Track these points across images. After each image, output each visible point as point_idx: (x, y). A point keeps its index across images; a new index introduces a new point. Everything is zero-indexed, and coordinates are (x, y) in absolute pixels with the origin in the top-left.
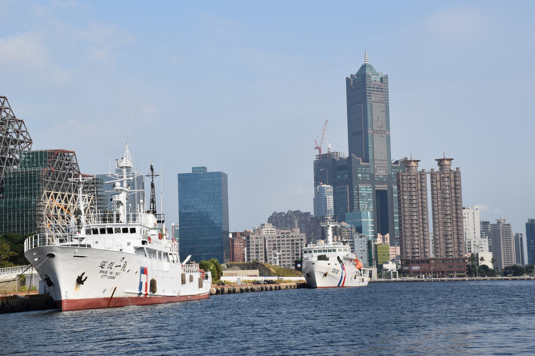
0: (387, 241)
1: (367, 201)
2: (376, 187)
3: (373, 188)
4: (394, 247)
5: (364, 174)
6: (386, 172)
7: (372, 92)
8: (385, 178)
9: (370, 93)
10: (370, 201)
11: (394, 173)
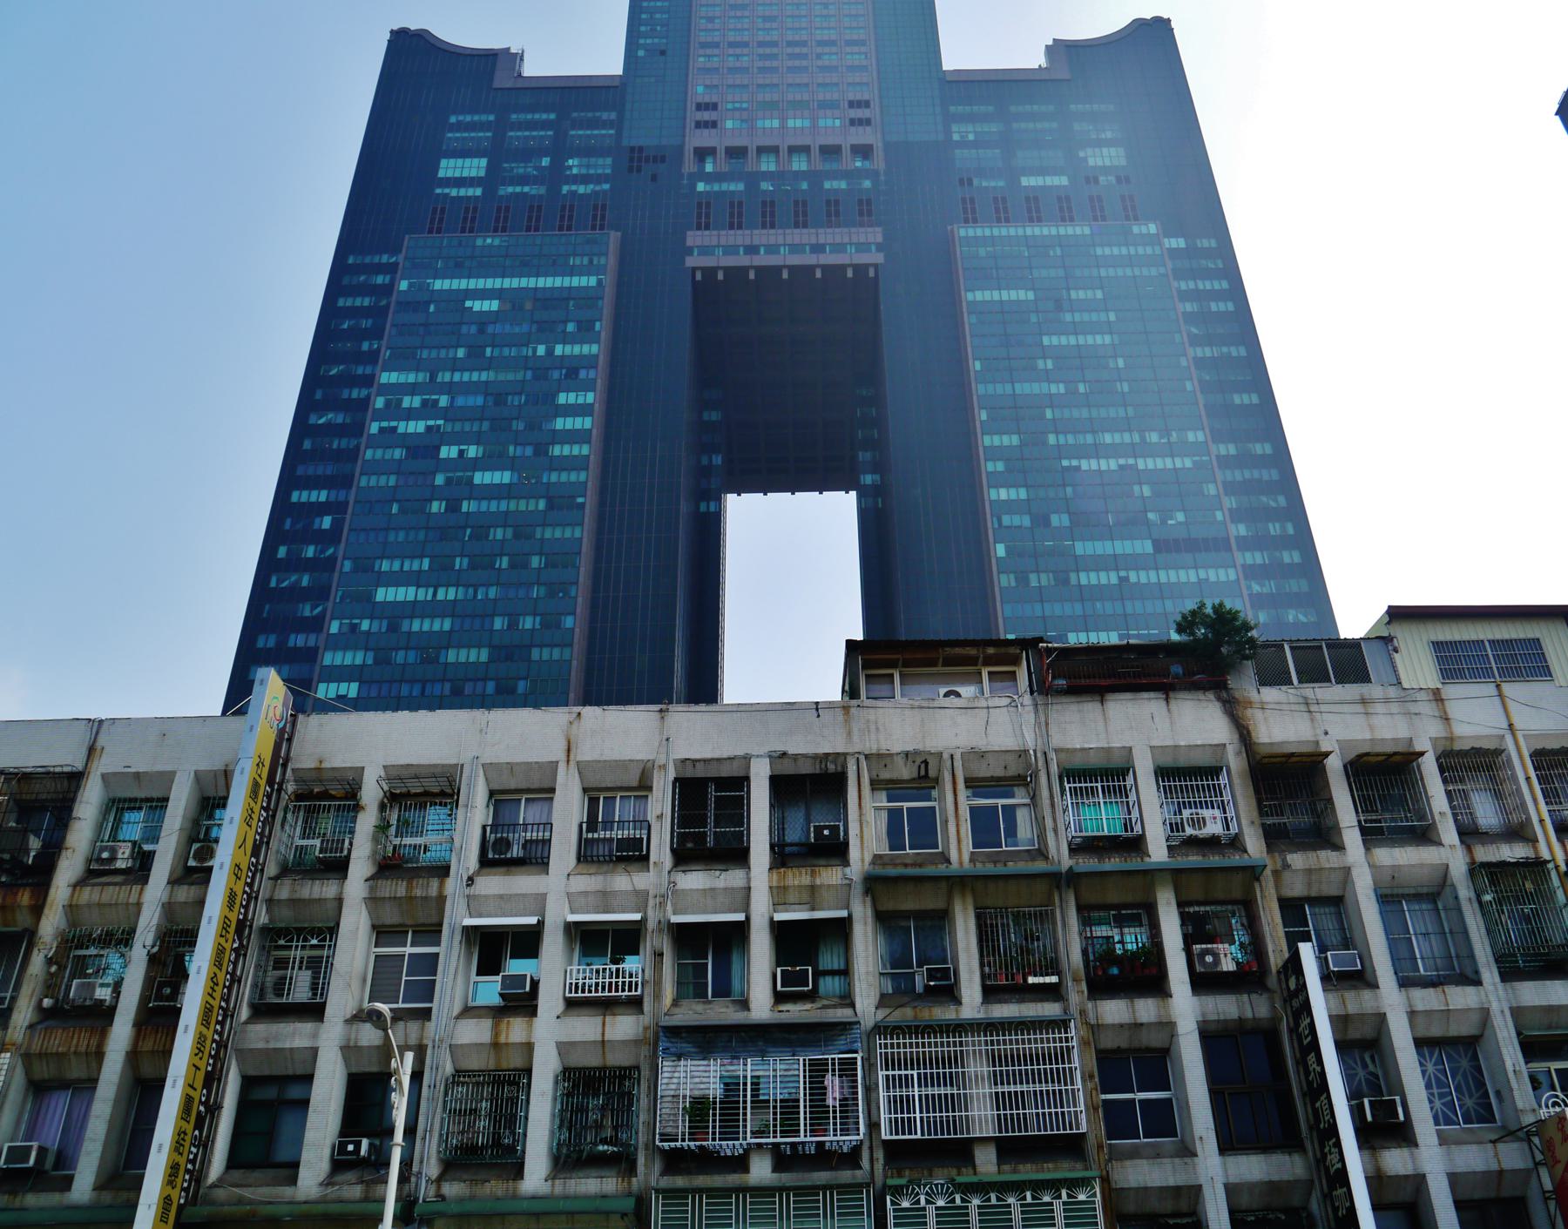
2: (705, 251)
5: (526, 154)
10: (572, 372)
11: (994, 128)
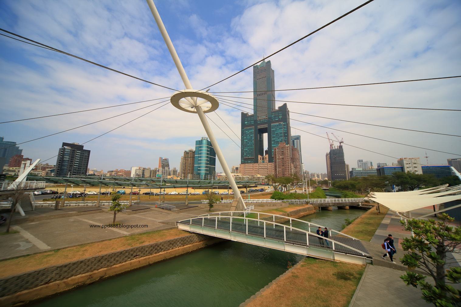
0: (266, 159)
1: (250, 136)
3: (256, 128)
4: (271, 163)
6: (267, 116)
7: (257, 74)
8: (266, 120)
9: (256, 75)
10: (253, 136)
